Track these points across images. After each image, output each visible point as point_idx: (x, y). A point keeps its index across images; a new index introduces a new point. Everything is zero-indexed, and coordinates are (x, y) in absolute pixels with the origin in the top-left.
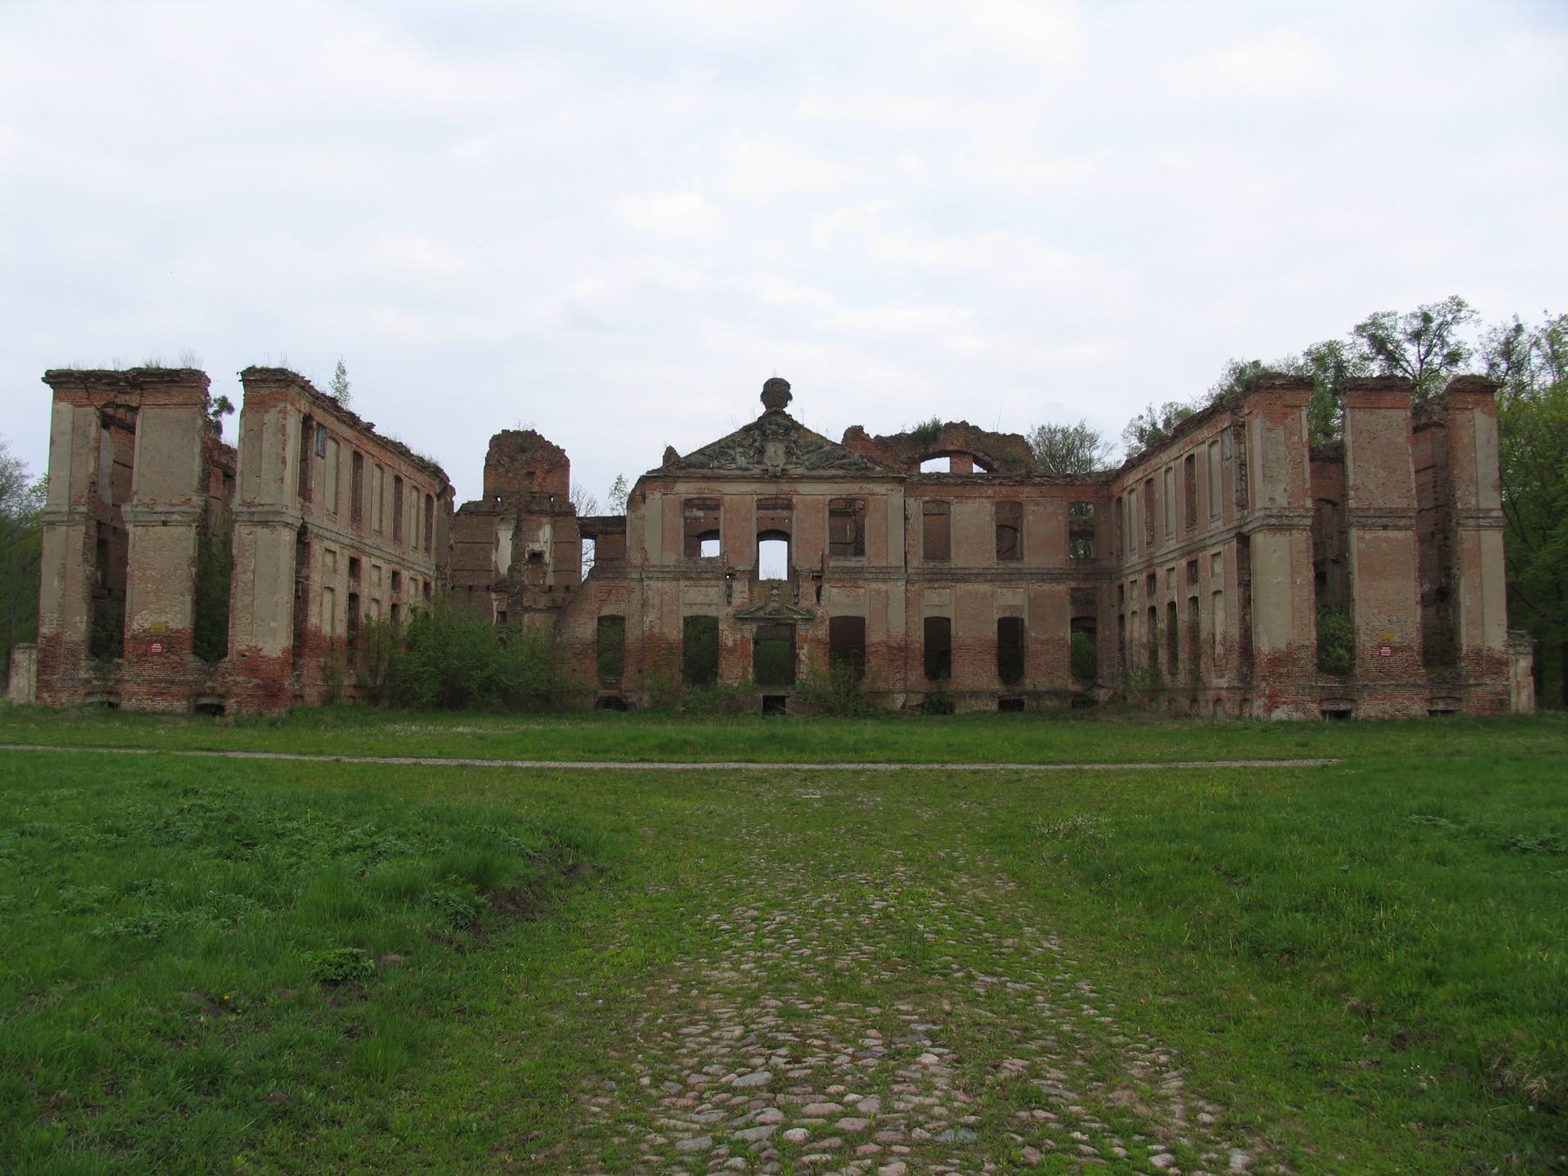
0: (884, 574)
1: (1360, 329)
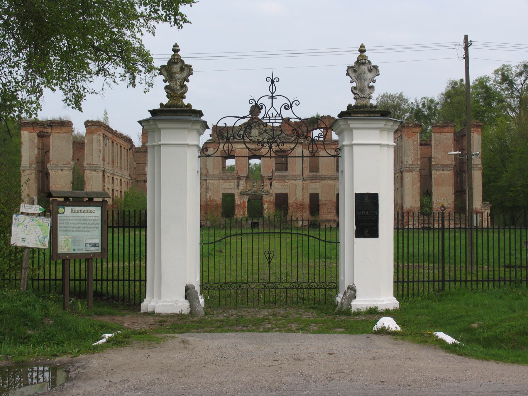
0: (295, 177)
1: (496, 72)
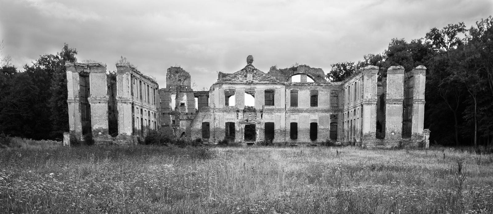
0: (279, 110)
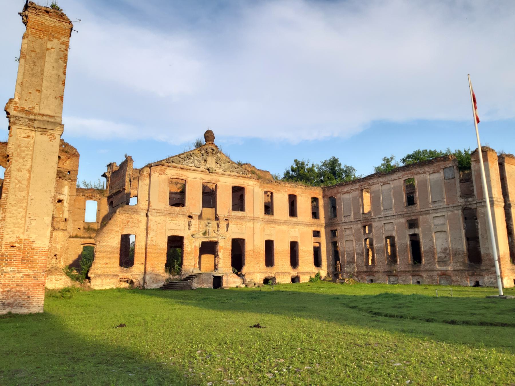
0: (253, 219)
